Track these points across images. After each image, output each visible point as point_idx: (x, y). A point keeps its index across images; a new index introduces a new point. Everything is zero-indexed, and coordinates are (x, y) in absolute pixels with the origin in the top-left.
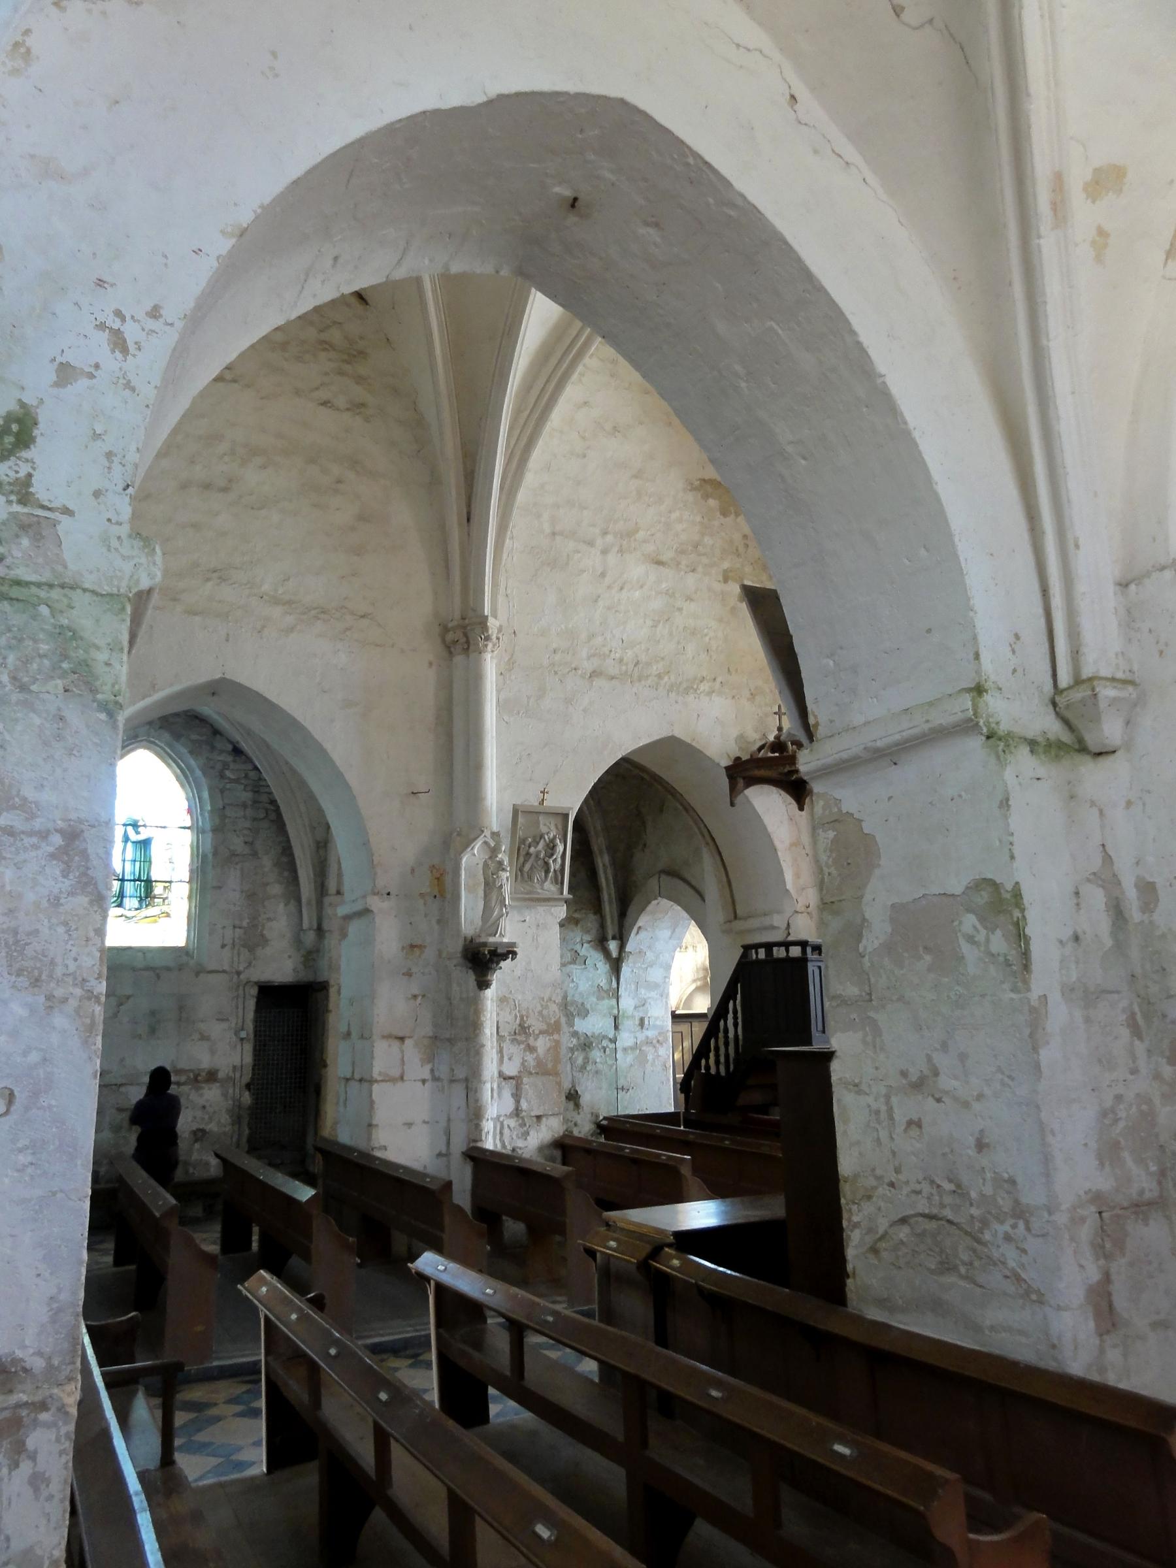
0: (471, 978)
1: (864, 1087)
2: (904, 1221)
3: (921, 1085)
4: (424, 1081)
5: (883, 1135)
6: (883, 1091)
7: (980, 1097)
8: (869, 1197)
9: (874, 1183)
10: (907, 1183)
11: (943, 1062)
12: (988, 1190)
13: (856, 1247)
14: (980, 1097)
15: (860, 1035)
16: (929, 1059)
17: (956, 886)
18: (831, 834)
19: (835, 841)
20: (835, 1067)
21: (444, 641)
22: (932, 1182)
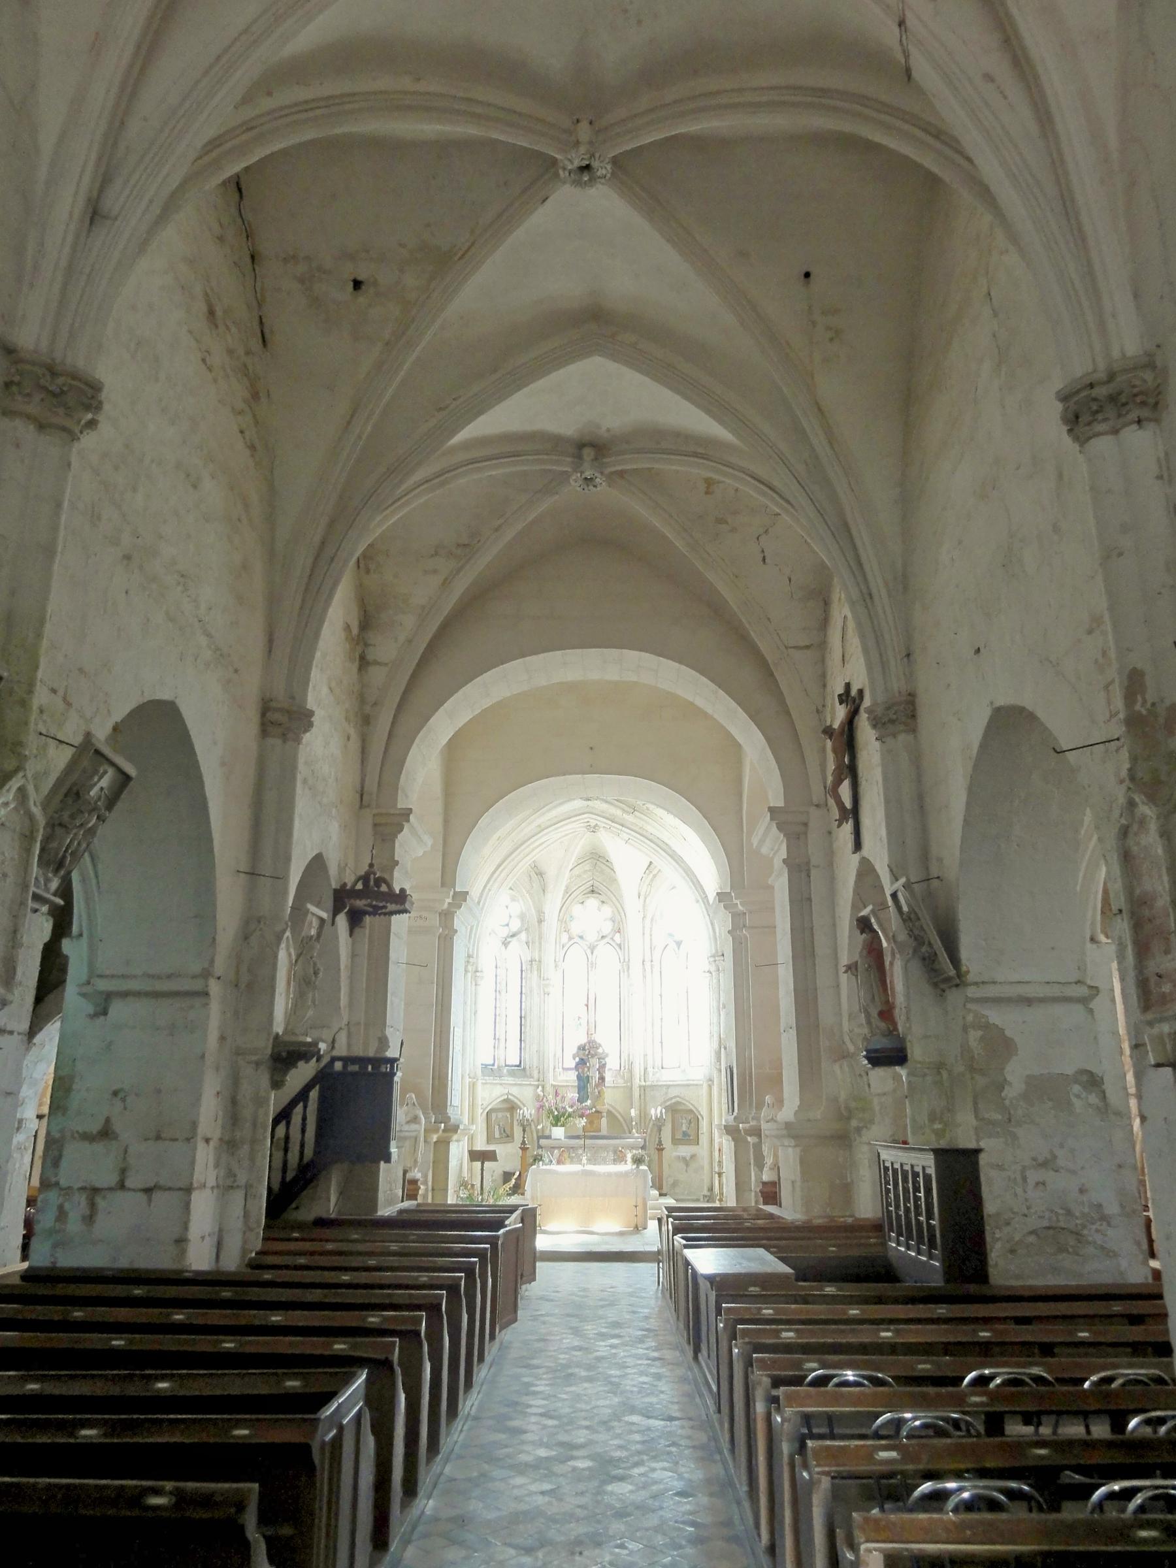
0: (264, 1079)
2: (1031, 1233)
3: (1047, 1163)
4: (213, 1188)
5: (1019, 1190)
7: (1082, 1168)
8: (1008, 1224)
10: (1036, 1212)
11: (1060, 1153)
12: (1086, 1210)
14: (1082, 1168)
15: (1002, 1140)
16: (1051, 1152)
17: (1070, 1070)
18: (980, 1033)
19: (982, 1039)
20: (983, 1159)
21: (263, 715)
22: (1052, 1211)
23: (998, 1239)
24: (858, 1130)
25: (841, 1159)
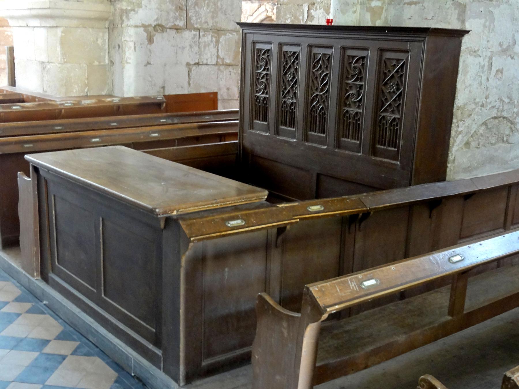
1: (480, 53)
5: (484, 78)
6: (489, 54)
9: (473, 106)
13: (458, 145)
15: (483, 21)
23: (461, 133)
24: (125, 13)
25: (100, 41)
